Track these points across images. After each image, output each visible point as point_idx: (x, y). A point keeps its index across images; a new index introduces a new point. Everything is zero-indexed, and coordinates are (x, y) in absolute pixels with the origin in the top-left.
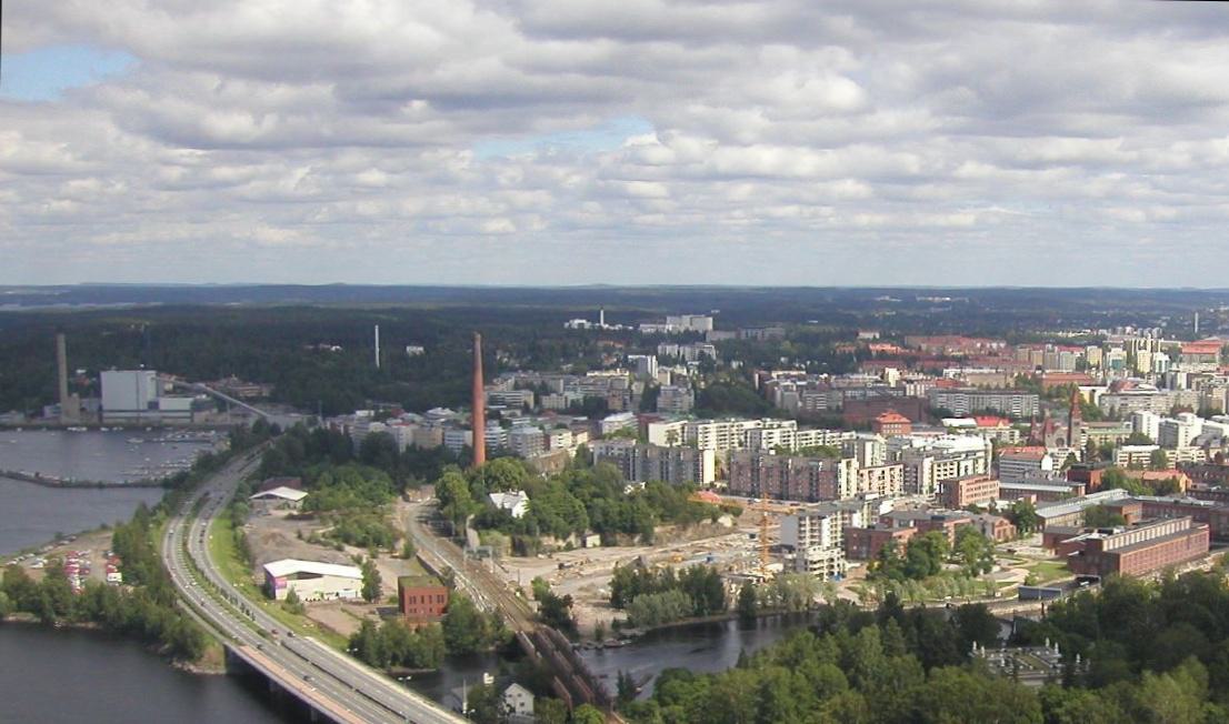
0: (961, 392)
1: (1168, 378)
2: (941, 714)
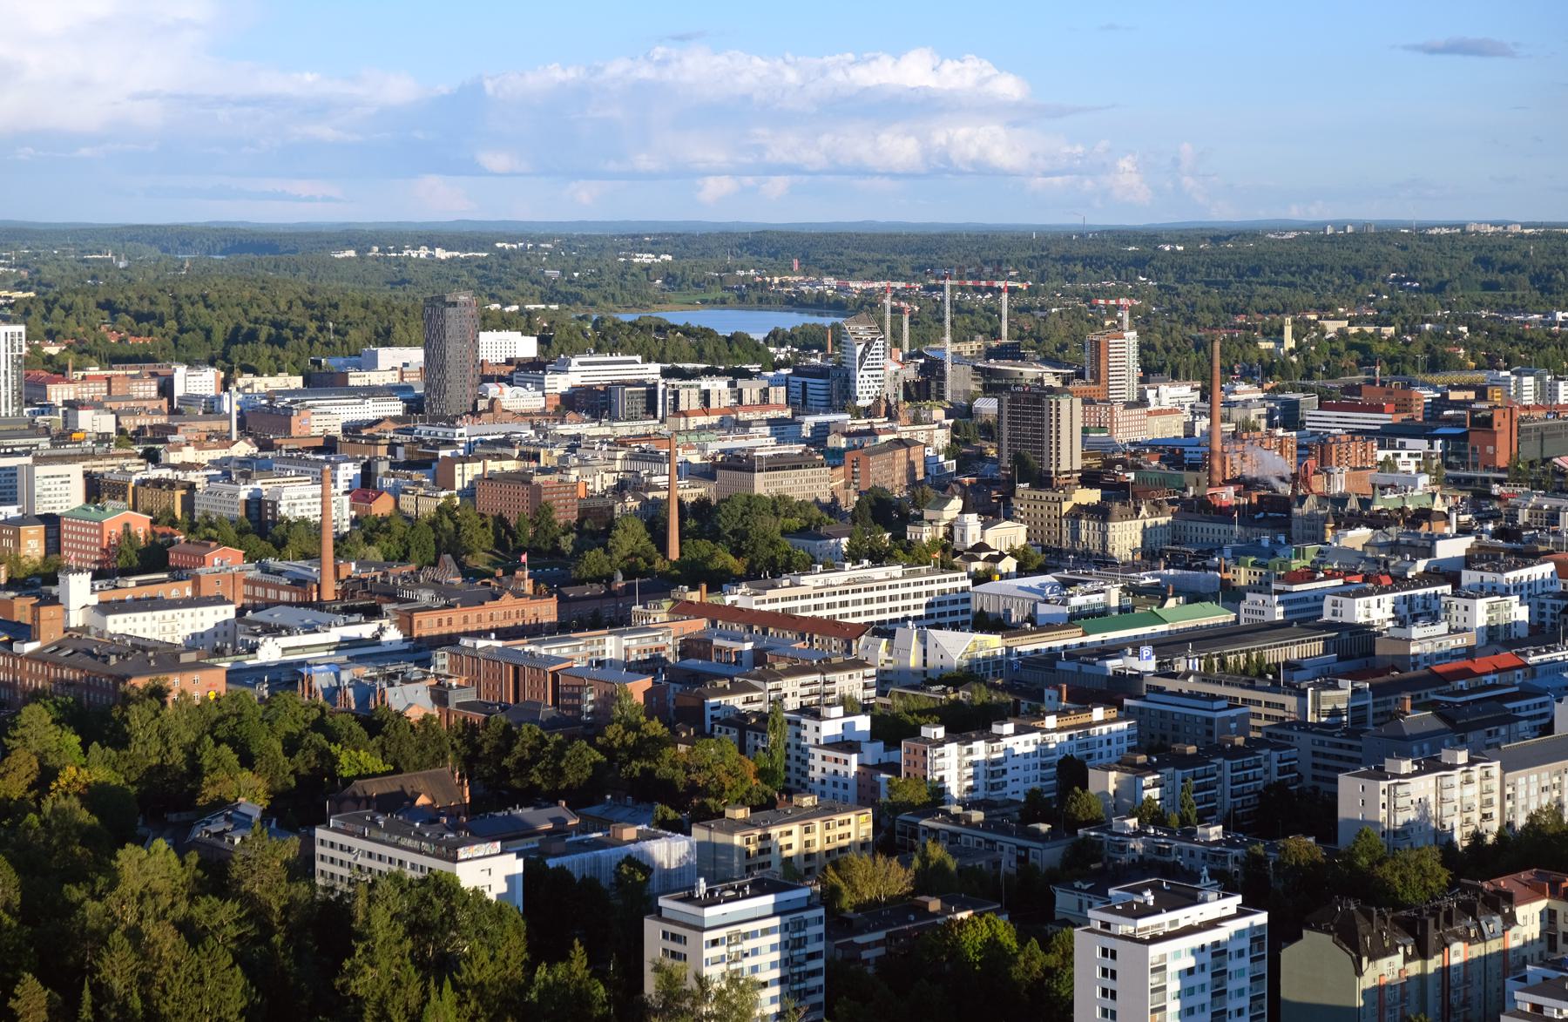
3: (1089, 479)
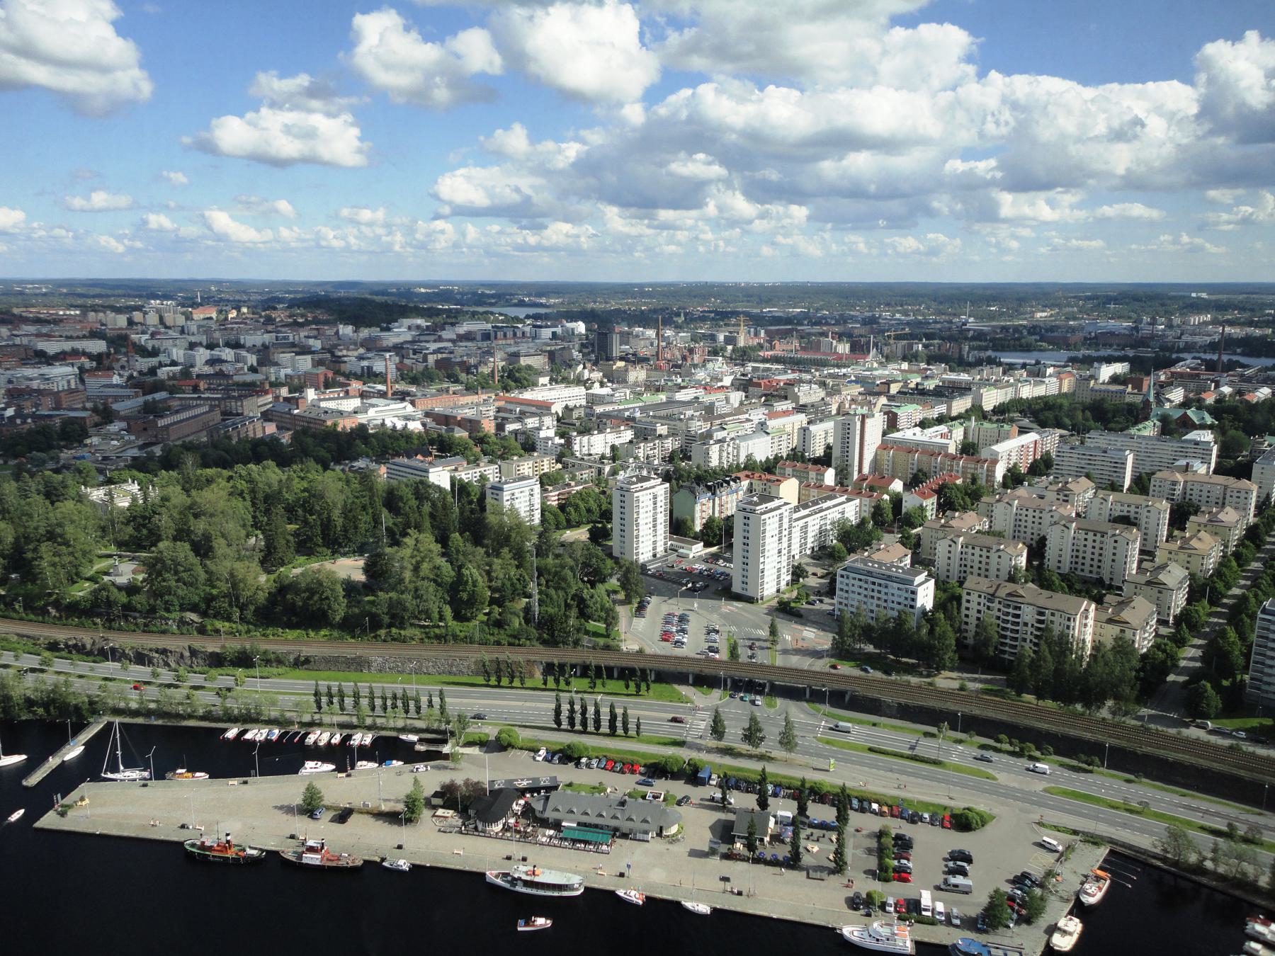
3: (622, 359)
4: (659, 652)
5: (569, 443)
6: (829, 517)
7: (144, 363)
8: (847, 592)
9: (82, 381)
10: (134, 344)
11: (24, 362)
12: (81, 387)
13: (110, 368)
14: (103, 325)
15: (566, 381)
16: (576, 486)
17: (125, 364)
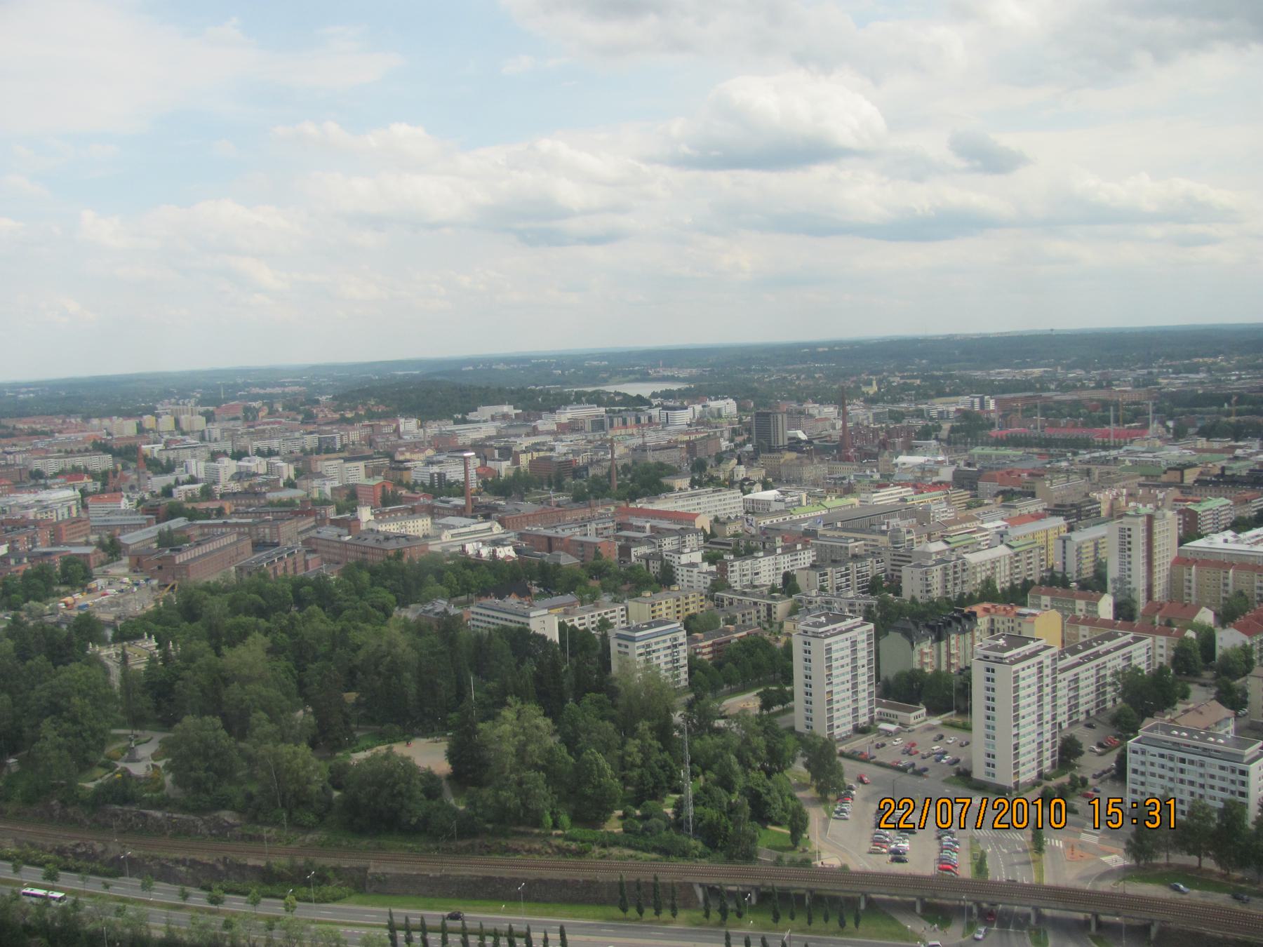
0: (51, 457)
1: (207, 434)
2: (73, 700)
4: (870, 868)
5: (723, 570)
6: (1109, 665)
7: (158, 482)
8: (1143, 774)
9: (85, 507)
10: (145, 457)
11: (18, 486)
12: (83, 515)
13: (117, 490)
14: (109, 434)
15: (714, 482)
16: (737, 631)
17: (135, 483)
